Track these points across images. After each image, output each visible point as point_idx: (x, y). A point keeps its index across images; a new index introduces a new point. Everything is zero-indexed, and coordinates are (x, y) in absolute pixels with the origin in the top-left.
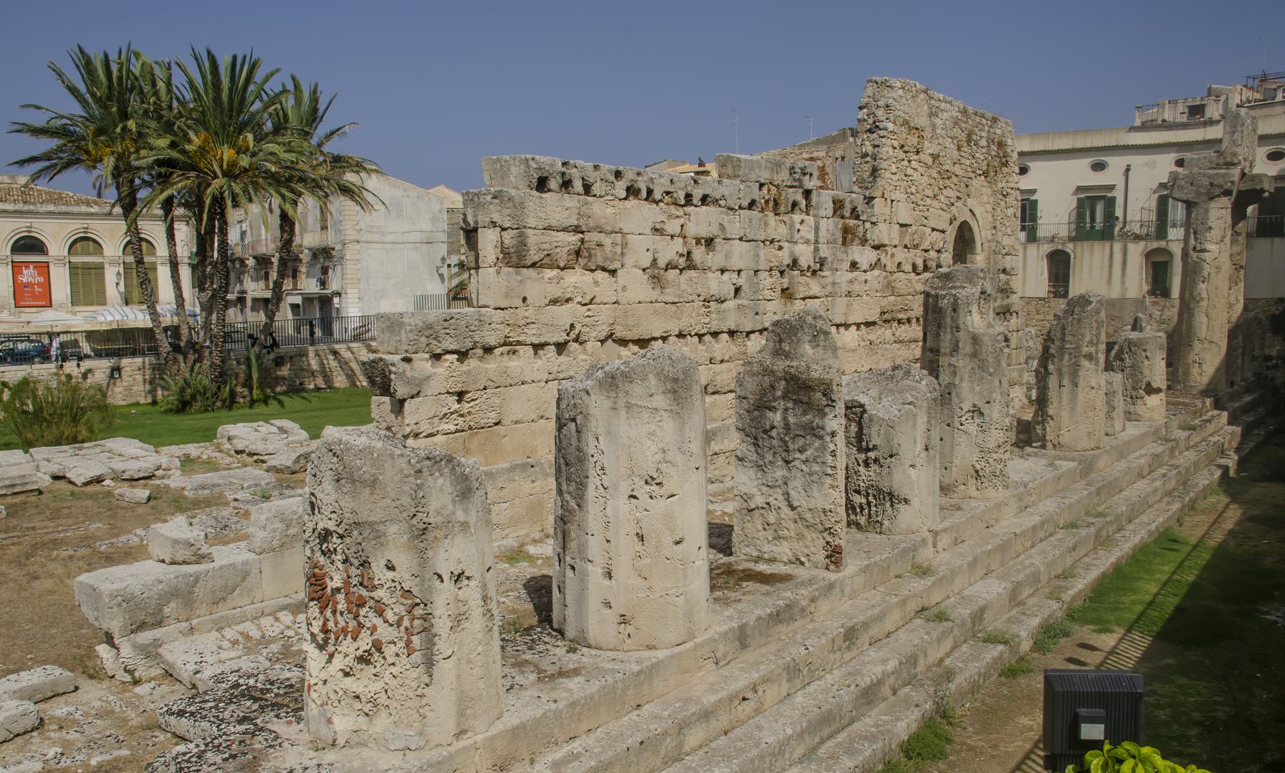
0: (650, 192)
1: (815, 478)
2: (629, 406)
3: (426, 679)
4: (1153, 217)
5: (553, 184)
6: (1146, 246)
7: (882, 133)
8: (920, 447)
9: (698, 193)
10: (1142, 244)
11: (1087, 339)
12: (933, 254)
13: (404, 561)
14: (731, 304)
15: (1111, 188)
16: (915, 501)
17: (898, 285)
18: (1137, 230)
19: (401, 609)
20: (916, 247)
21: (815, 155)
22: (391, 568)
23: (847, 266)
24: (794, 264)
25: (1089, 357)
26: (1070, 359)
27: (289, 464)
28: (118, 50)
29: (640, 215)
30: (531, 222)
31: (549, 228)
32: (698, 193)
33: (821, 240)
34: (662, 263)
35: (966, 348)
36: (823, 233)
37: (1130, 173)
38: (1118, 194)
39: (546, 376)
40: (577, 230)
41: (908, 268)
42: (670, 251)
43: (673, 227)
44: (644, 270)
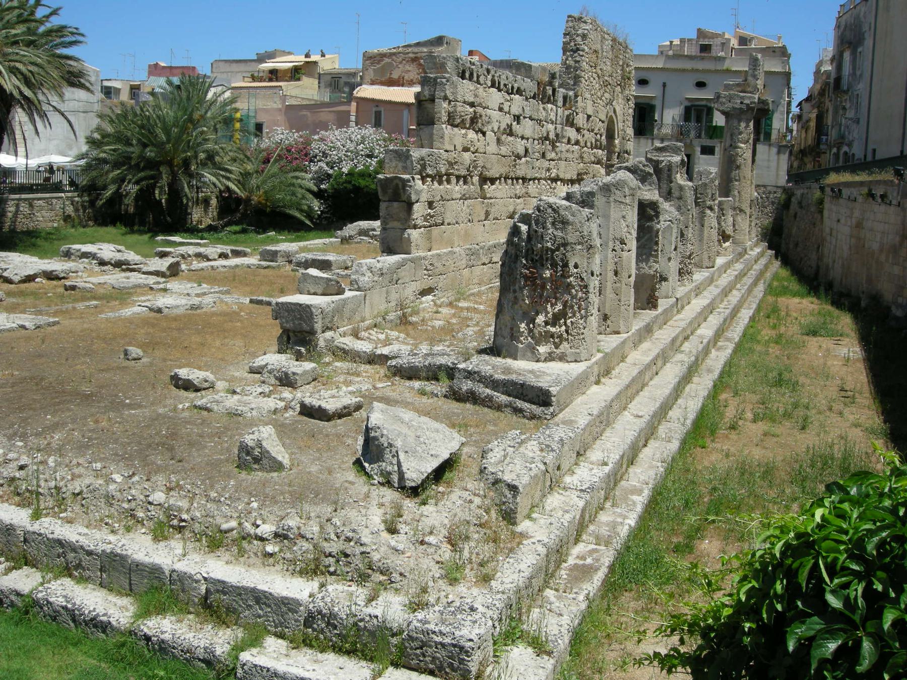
0: (499, 83)
5: (467, 75)
7: (581, 53)
8: (673, 247)
9: (516, 86)
14: (523, 159)
16: (670, 279)
17: (585, 156)
20: (593, 131)
21: (419, 55)
22: (576, 266)
23: (565, 140)
24: (547, 138)
25: (711, 208)
27: (164, 269)
29: (495, 97)
30: (460, 98)
31: (464, 102)
32: (516, 86)
34: (502, 129)
35: (676, 193)
39: (459, 196)
40: (472, 105)
41: (589, 144)
43: (506, 109)
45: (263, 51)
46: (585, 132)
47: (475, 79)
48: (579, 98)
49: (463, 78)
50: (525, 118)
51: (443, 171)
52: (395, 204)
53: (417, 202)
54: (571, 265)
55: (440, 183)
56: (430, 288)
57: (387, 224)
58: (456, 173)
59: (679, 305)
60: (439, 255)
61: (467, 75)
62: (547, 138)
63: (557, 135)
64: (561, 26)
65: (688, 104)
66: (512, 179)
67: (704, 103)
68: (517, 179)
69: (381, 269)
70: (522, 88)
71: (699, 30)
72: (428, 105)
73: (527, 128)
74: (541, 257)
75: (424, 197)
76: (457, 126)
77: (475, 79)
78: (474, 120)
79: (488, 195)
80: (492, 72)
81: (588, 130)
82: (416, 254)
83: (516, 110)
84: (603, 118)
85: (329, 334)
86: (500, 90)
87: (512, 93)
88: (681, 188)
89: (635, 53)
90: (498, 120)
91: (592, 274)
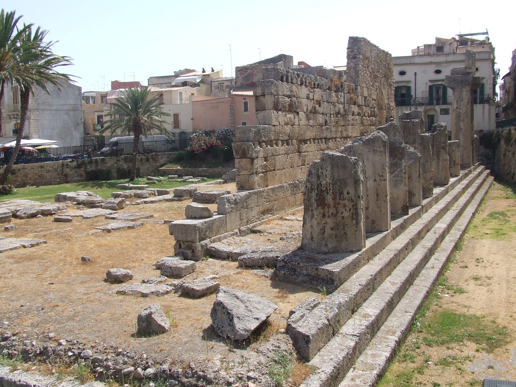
0: (305, 82)
1: (398, 182)
2: (374, 150)
3: (356, 229)
4: (427, 95)
5: (285, 79)
6: (425, 108)
9: (317, 83)
10: (423, 107)
11: (442, 141)
12: (373, 109)
13: (352, 191)
15: (409, 82)
18: (421, 101)
19: (351, 207)
24: (339, 113)
26: (436, 149)
28: (20, 15)
29: (304, 91)
30: (280, 93)
31: (284, 95)
32: (317, 83)
33: (346, 103)
34: (309, 109)
36: (346, 100)
37: (417, 76)
38: (412, 85)
40: (289, 97)
41: (366, 114)
42: (310, 104)
43: (311, 97)
44: (305, 113)
45: (177, 70)
46: (364, 107)
47: (290, 81)
48: (359, 87)
49: (282, 81)
50: (324, 102)
51: (273, 138)
52: (244, 160)
53: (257, 158)
54: (345, 193)
55: (272, 146)
56: (268, 209)
57: (240, 172)
58: (281, 138)
59: (425, 209)
60: (272, 189)
61: (285, 79)
62: (339, 113)
63: (345, 111)
64: (345, 44)
65: (430, 84)
66: (318, 139)
67: (440, 83)
68: (321, 139)
69: (235, 200)
70: (321, 84)
71: (437, 38)
72: (262, 98)
73: (324, 108)
74: (326, 188)
75: (261, 155)
76: (280, 110)
77: (290, 81)
78: (291, 106)
79: (303, 150)
80: (301, 76)
81: (365, 106)
82: (258, 189)
83: (316, 97)
84: (375, 98)
85: (203, 242)
86: (306, 86)
87: (314, 88)
88: (422, 137)
89: (392, 56)
90: (306, 104)
91: (359, 197)
